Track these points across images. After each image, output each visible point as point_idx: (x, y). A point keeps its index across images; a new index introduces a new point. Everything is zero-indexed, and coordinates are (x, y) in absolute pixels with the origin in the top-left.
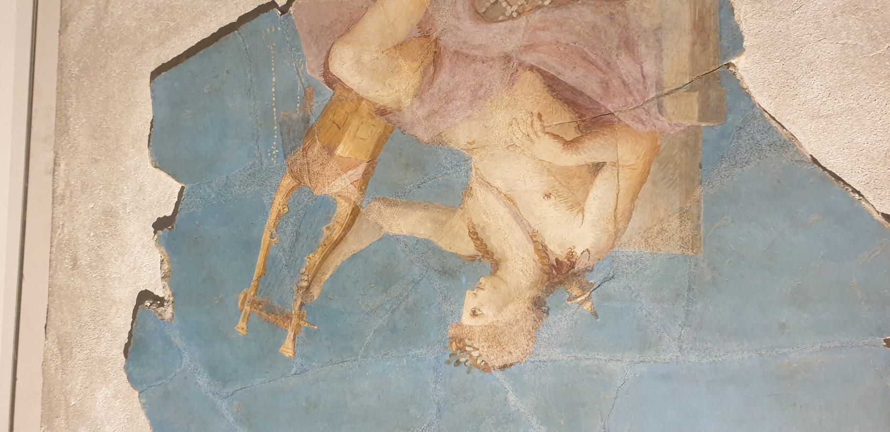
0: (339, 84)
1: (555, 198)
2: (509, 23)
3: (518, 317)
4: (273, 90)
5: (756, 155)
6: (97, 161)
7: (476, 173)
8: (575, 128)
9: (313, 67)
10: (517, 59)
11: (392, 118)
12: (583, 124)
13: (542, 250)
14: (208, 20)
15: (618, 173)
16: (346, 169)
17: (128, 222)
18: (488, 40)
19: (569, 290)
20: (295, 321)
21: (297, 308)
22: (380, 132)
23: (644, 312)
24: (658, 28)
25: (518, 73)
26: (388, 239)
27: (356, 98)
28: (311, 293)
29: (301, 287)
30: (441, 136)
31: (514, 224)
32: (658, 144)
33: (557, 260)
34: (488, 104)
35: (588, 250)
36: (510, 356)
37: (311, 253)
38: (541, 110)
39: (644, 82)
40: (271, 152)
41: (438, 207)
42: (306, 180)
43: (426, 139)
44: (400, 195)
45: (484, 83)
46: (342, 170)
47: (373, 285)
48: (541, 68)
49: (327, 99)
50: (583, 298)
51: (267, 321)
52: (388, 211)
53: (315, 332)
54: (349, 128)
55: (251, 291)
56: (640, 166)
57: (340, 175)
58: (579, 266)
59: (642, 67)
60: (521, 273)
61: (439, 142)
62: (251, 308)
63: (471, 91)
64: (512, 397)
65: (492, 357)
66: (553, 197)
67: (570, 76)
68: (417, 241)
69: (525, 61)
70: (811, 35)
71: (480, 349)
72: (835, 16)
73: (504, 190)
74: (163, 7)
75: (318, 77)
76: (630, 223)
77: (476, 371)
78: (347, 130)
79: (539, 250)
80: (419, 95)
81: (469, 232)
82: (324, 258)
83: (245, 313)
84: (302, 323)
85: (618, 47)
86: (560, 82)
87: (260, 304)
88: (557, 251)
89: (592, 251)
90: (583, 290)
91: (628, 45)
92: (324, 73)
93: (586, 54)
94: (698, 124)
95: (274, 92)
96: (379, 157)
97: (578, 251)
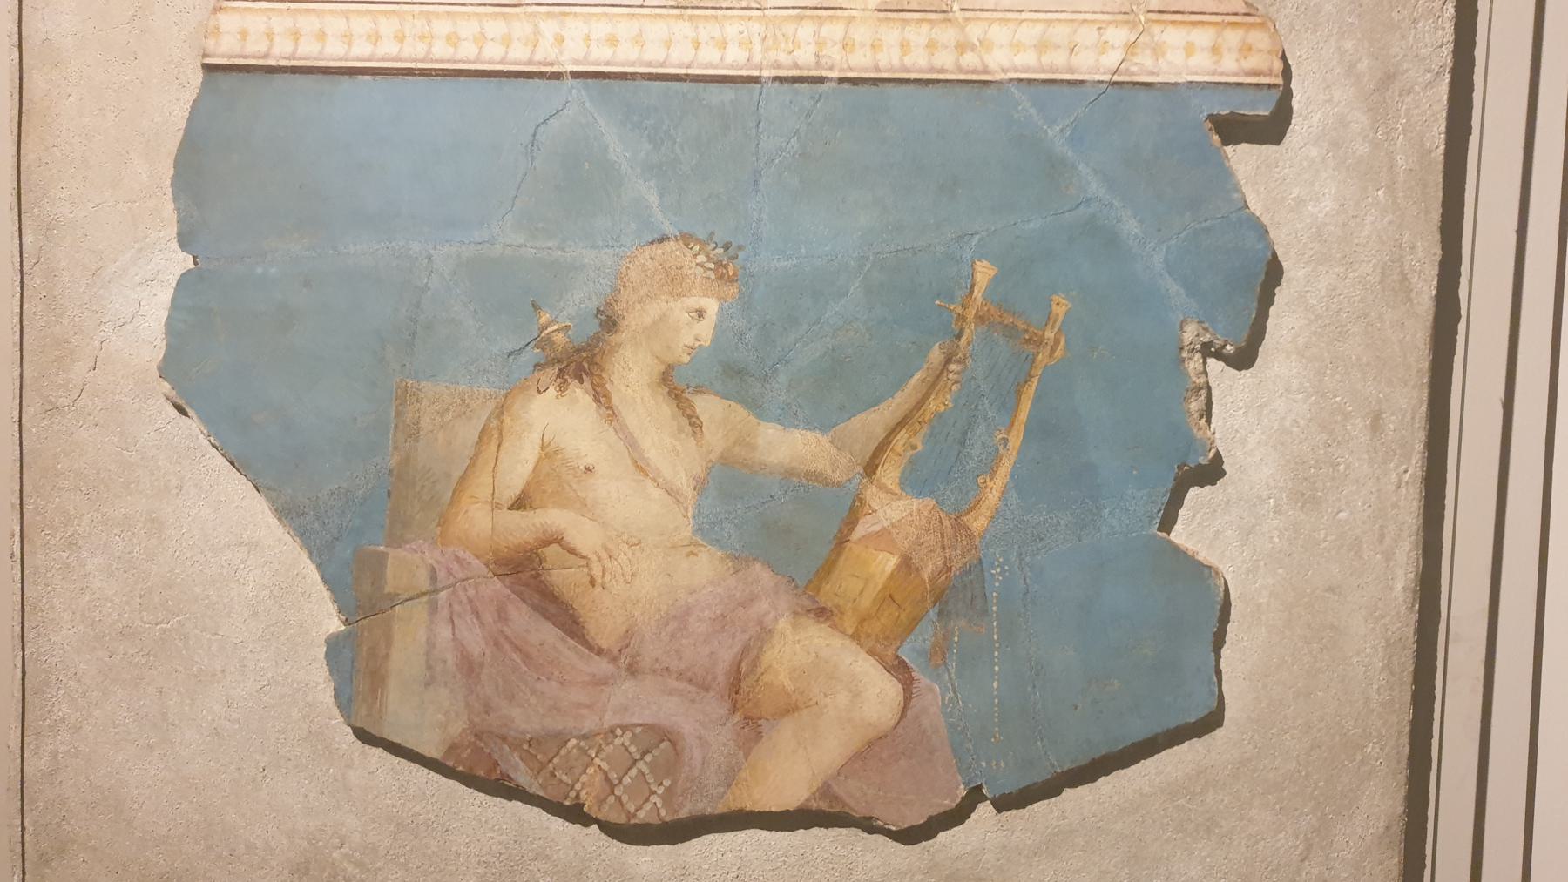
0: (887, 663)
1: (579, 467)
2: (627, 720)
3: (639, 307)
4: (997, 668)
5: (321, 503)
6: (1331, 589)
7: (686, 510)
8: (546, 561)
10: (619, 667)
11: (808, 603)
12: (535, 565)
13: (601, 396)
14: (1115, 799)
15: (493, 494)
16: (883, 534)
17: (1272, 484)
19: (567, 340)
20: (971, 313)
21: (967, 332)
22: (828, 583)
23: (472, 308)
24: (429, 685)
26: (824, 428)
27: (862, 640)
28: (944, 353)
29: (958, 362)
30: (734, 568)
32: (439, 528)
33: (581, 381)
35: (540, 392)
37: (943, 413)
38: (591, 591)
39: (452, 613)
42: (946, 523)
43: (758, 566)
44: (802, 489)
46: (890, 533)
47: (847, 360)
48: (586, 651)
49: (909, 643)
50: (549, 330)
51: (1016, 316)
52: (822, 465)
54: (874, 595)
55: (1043, 360)
57: (893, 525)
58: (552, 371)
59: (454, 634)
60: (631, 365)
61: (739, 560)
62: (1044, 334)
64: (653, 199)
65: (678, 253)
66: (582, 467)
67: (546, 634)
68: (779, 420)
69: (609, 663)
70: (251, 651)
71: (693, 265)
72: (223, 671)
73: (649, 483)
74: (1198, 834)
75: (923, 679)
76: (482, 425)
77: (702, 235)
78: (880, 591)
80: (765, 633)
81: (701, 427)
82: (920, 404)
83: (1053, 327)
84: (959, 310)
85: (482, 665)
86: (561, 626)
87: (1028, 341)
88: (580, 394)
90: (548, 339)
91: (469, 667)
92: (912, 684)
94: (389, 550)
95: (995, 665)
97: (552, 391)
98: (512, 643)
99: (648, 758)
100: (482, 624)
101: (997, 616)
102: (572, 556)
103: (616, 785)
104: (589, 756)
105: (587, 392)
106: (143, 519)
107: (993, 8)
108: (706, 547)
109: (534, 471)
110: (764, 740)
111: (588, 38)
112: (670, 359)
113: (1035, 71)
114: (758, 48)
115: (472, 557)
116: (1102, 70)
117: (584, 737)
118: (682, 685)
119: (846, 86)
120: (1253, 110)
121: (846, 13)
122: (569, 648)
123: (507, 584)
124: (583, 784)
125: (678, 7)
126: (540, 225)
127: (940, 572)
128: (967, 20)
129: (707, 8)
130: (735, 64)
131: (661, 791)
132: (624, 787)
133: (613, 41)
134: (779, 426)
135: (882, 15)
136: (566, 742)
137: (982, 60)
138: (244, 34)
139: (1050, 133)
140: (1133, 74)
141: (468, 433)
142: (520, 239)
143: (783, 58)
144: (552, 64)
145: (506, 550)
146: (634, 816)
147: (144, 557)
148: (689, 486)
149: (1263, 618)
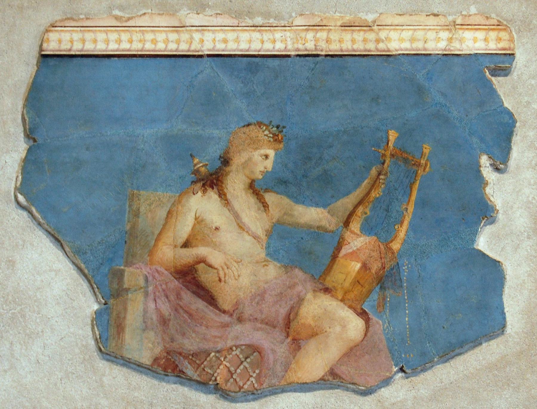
0: (358, 312)
2: (238, 343)
4: (407, 312)
9: (378, 326)
11: (321, 286)
13: (222, 195)
14: (465, 372)
17: (525, 225)
18: (253, 333)
20: (388, 153)
21: (387, 161)
25: (233, 309)
26: (325, 206)
31: (239, 211)
33: (213, 188)
34: (253, 291)
35: (194, 194)
36: (245, 132)
39: (155, 296)
40: (408, 267)
41: (290, 224)
42: (382, 247)
43: (297, 270)
44: (316, 234)
45: (255, 305)
46: (356, 253)
48: (218, 312)
50: (198, 166)
51: (408, 154)
52: (324, 223)
53: (374, 146)
55: (420, 173)
56: (160, 244)
58: (200, 185)
59: (156, 306)
60: (236, 181)
61: (288, 267)
63: (264, 300)
66: (214, 228)
67: (199, 305)
69: (229, 317)
71: (263, 135)
72: (42, 332)
77: (267, 123)
78: (353, 279)
80: (301, 300)
81: (268, 207)
82: (368, 193)
83: (424, 158)
84: (383, 152)
85: (169, 320)
87: (414, 165)
88: (213, 195)
89: (192, 194)
92: (369, 320)
93: (189, 318)
96: (330, 260)
97: (200, 194)
98: (183, 309)
99: (248, 360)
100: (169, 301)
101: (407, 288)
102: (211, 269)
103: (233, 374)
104: (221, 360)
105: (215, 193)
106: (5, 261)
107: (390, 24)
108: (272, 262)
109: (192, 229)
110: (302, 349)
111: (214, 40)
112: (253, 177)
113: (410, 50)
114: (289, 43)
115: (164, 270)
116: (438, 49)
117: (218, 352)
118: (263, 326)
119: (328, 58)
120: (504, 64)
121: (327, 28)
123: (181, 282)
124: (218, 373)
125: (253, 26)
126: (194, 120)
127: (381, 269)
128: (380, 30)
129: (266, 27)
130: (279, 50)
131: (254, 375)
132: (238, 374)
133: (225, 41)
134: (304, 206)
135: (343, 28)
136: (209, 355)
137: (387, 46)
138: (60, 41)
139: (418, 76)
140: (452, 50)
141: (162, 213)
142: (185, 127)
143: (300, 46)
144: (198, 51)
145: (180, 267)
146: (242, 387)
147: (5, 279)
148: (263, 235)
149: (526, 286)
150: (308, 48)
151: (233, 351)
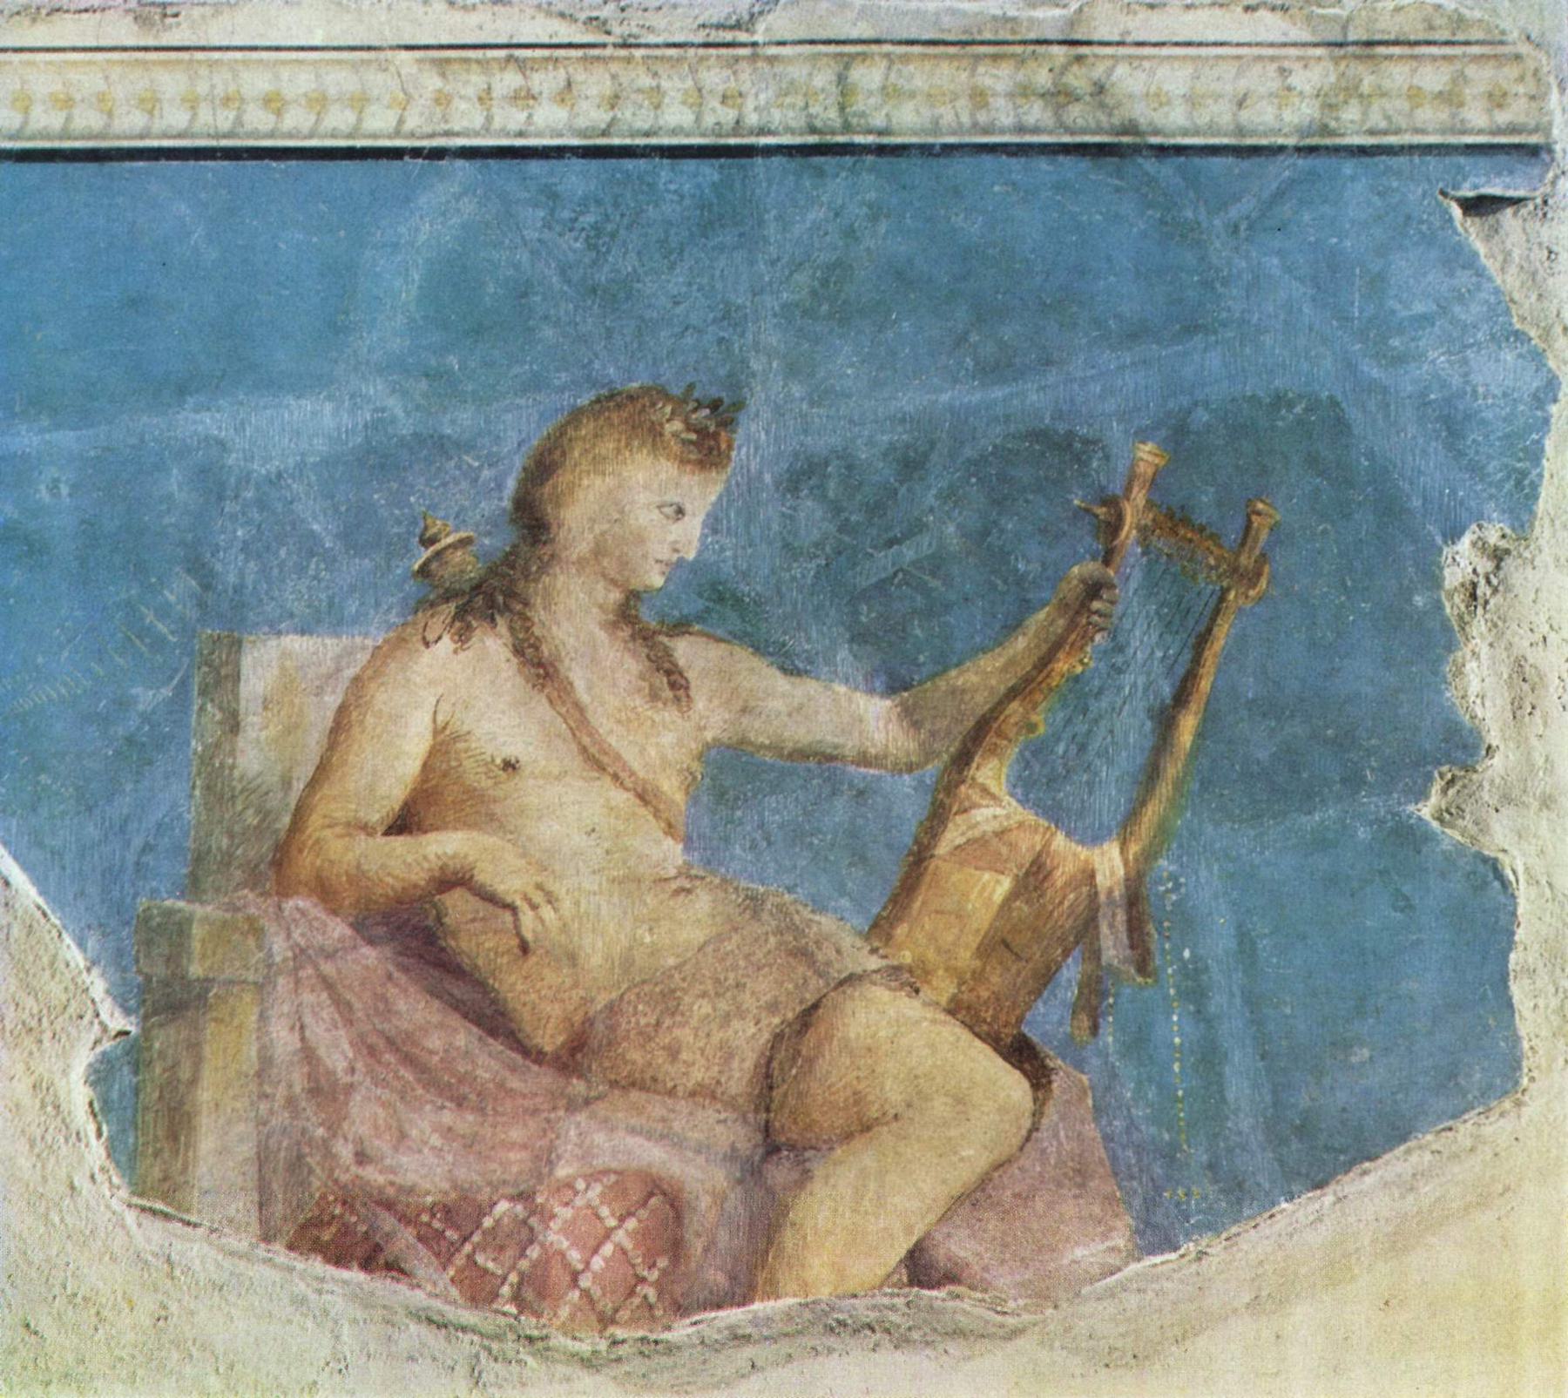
1: (493, 761)
35: (427, 644)
59: (303, 1039)
66: (498, 761)
79: (531, 646)
81: (687, 688)
88: (493, 644)
97: (447, 644)
99: (631, 1224)
122: (490, 1055)
131: (654, 1275)
150: (818, 124)
151: (576, 1193)
